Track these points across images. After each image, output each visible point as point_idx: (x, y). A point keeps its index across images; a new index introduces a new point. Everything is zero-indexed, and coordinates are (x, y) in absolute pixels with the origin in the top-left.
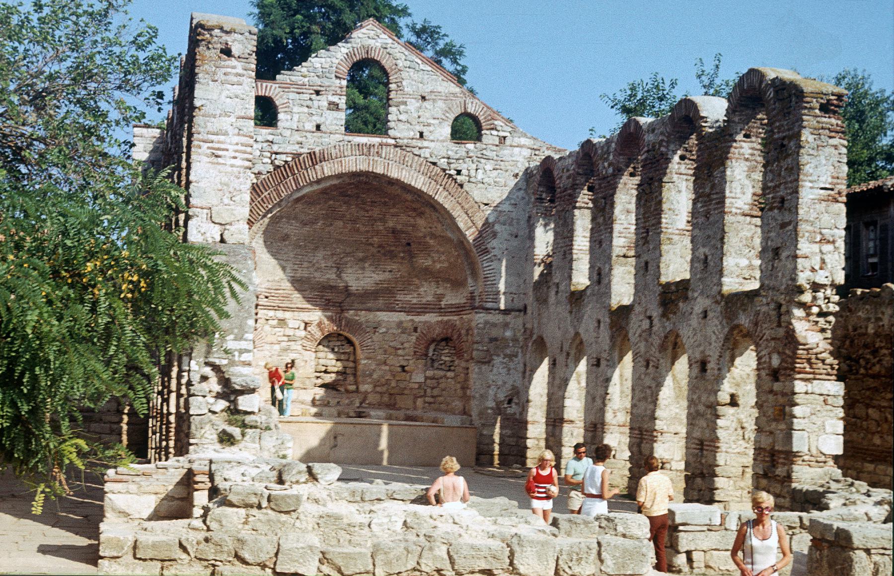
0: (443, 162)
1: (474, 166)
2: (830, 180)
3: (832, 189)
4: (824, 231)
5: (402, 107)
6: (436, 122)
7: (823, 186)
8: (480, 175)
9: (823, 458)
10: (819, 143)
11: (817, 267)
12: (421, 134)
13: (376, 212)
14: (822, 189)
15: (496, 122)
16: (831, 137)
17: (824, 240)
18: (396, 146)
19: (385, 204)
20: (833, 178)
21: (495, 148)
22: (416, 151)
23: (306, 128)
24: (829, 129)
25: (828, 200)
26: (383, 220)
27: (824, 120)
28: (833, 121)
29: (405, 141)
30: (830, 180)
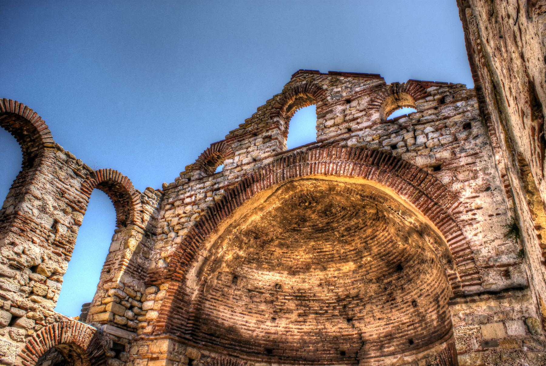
0: (375, 145)
1: (411, 134)
5: (329, 116)
6: (364, 113)
8: (421, 139)
12: (349, 130)
13: (358, 243)
15: (429, 90)
18: (321, 147)
19: (357, 228)
21: (432, 111)
22: (343, 143)
23: (244, 163)
26: (368, 248)
29: (332, 140)
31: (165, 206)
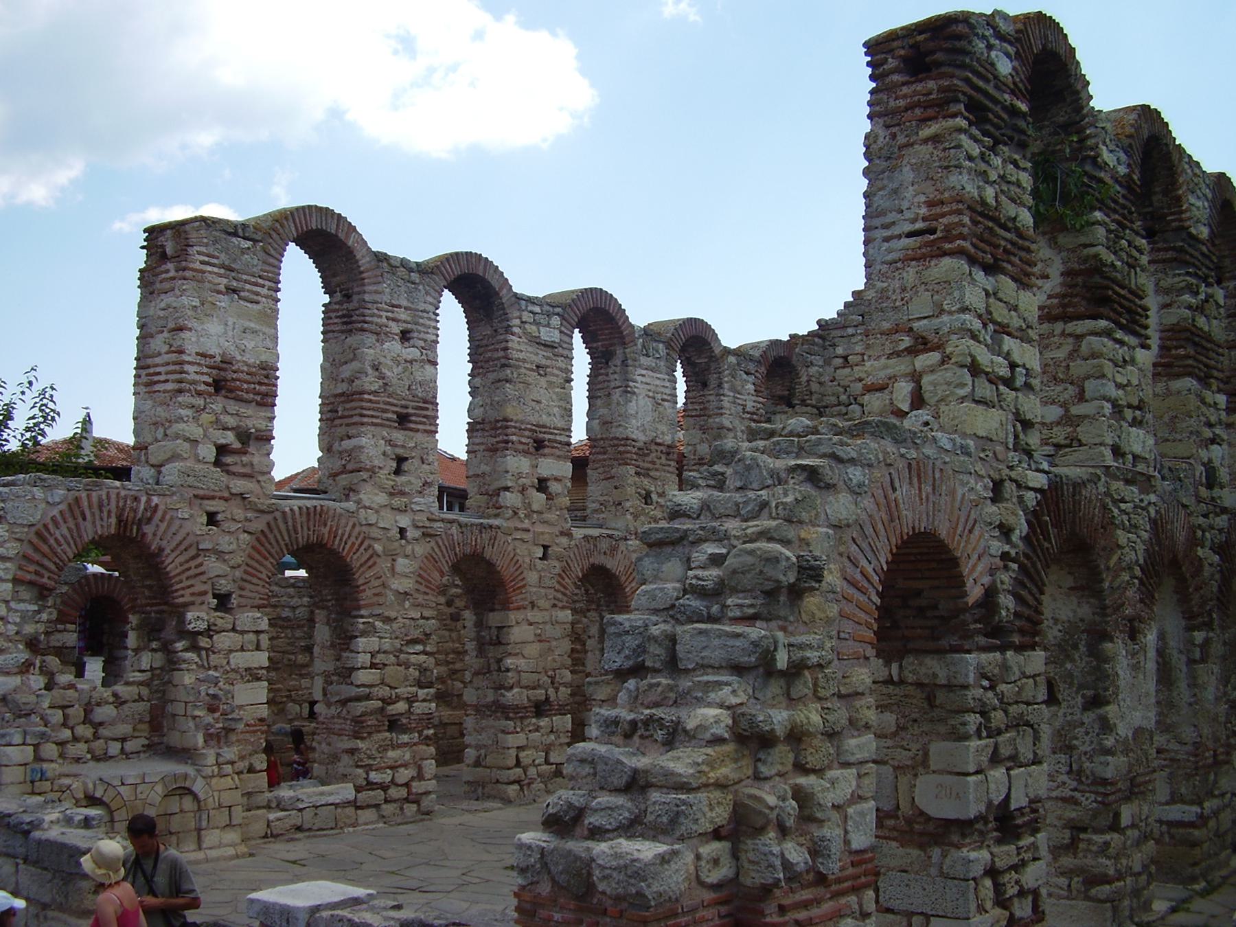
2: (923, 211)
3: (932, 231)
4: (916, 325)
7: (908, 228)
9: (931, 827)
10: (901, 139)
11: (905, 408)
14: (910, 235)
16: (924, 121)
17: (922, 344)
20: (930, 204)
24: (918, 105)
25: (923, 257)
27: (905, 90)
28: (931, 84)
30: (923, 211)
31: (831, 359)
